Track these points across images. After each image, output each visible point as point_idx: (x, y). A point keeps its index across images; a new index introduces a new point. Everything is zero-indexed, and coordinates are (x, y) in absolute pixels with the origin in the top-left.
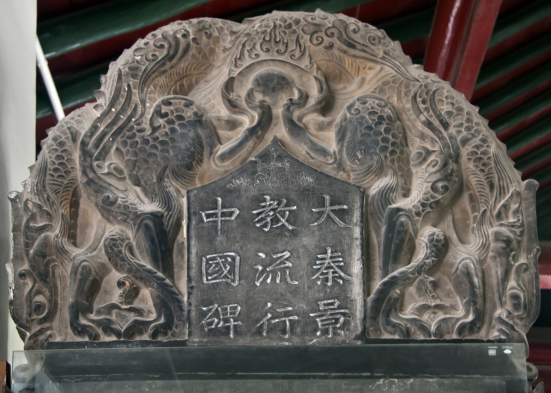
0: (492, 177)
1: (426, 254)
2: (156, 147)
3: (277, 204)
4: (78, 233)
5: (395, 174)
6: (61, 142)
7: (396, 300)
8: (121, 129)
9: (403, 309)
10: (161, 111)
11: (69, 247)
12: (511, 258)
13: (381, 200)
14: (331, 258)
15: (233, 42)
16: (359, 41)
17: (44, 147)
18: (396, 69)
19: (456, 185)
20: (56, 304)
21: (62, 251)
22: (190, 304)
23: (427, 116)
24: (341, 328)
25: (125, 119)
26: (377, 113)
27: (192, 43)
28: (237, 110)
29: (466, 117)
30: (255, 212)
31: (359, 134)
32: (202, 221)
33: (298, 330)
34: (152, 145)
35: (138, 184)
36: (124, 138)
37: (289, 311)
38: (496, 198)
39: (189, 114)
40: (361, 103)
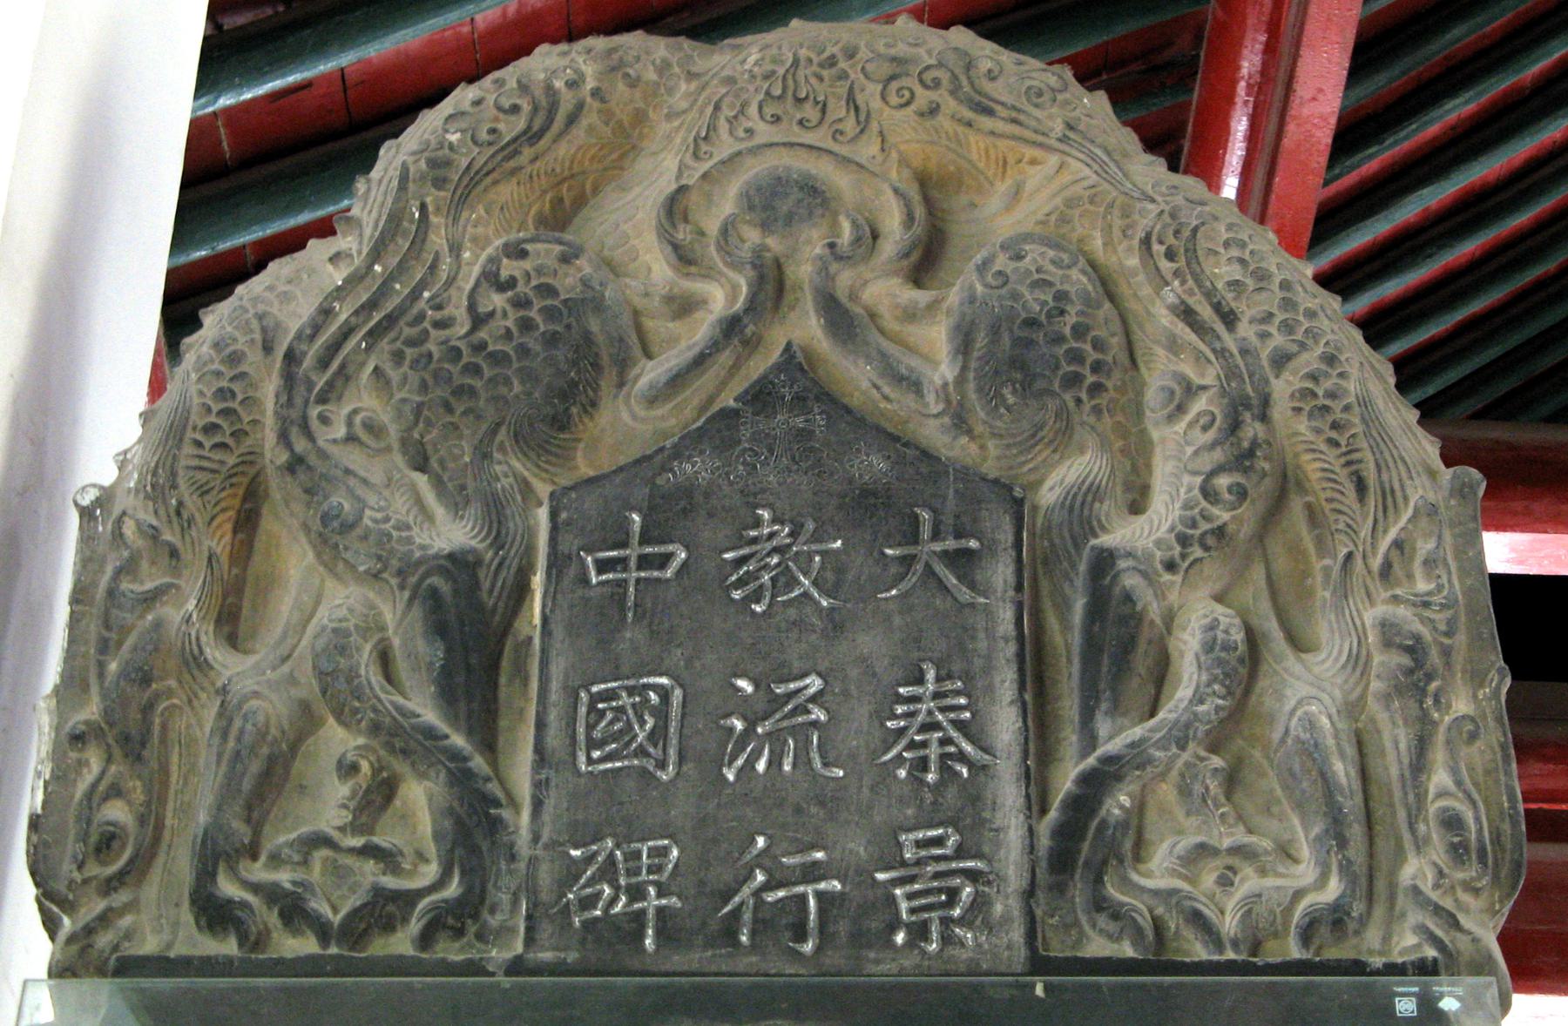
0: (1360, 461)
1: (1198, 686)
2: (475, 370)
3: (791, 534)
4: (246, 605)
5: (1104, 445)
6: (235, 352)
7: (1124, 825)
8: (391, 320)
9: (1143, 854)
10: (497, 275)
11: (215, 652)
12: (1429, 701)
13: (1071, 523)
14: (937, 696)
15: (693, 97)
16: (1003, 99)
17: (189, 359)
18: (1096, 167)
19: (1267, 481)
20: (159, 827)
21: (196, 663)
22: (536, 838)
23: (1179, 290)
24: (961, 921)
25: (406, 291)
26: (1051, 284)
27: (589, 99)
28: (693, 269)
29: (1280, 294)
30: (728, 556)
31: (1006, 340)
32: (585, 581)
33: (843, 928)
34: (468, 364)
35: (422, 466)
36: (398, 344)
37: (816, 863)
38: (1376, 521)
39: (569, 281)
40: (1011, 259)
